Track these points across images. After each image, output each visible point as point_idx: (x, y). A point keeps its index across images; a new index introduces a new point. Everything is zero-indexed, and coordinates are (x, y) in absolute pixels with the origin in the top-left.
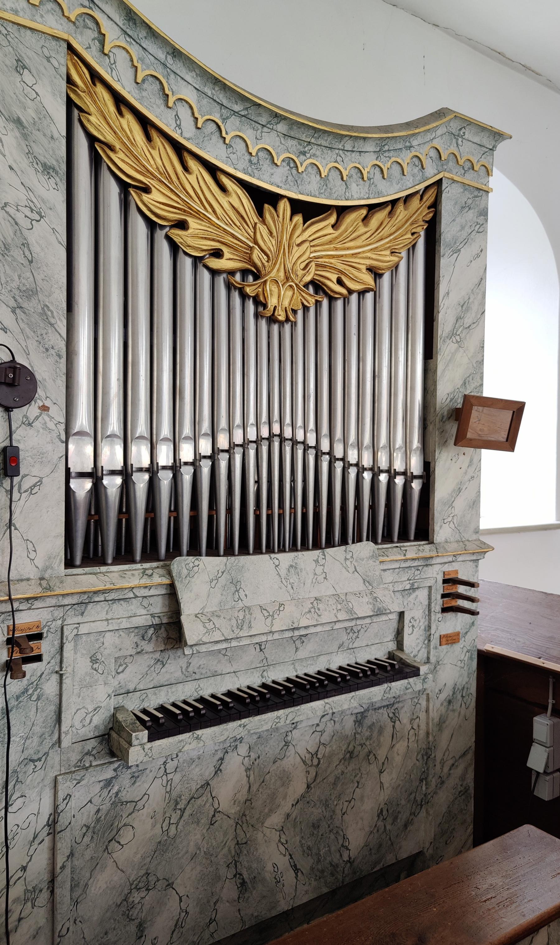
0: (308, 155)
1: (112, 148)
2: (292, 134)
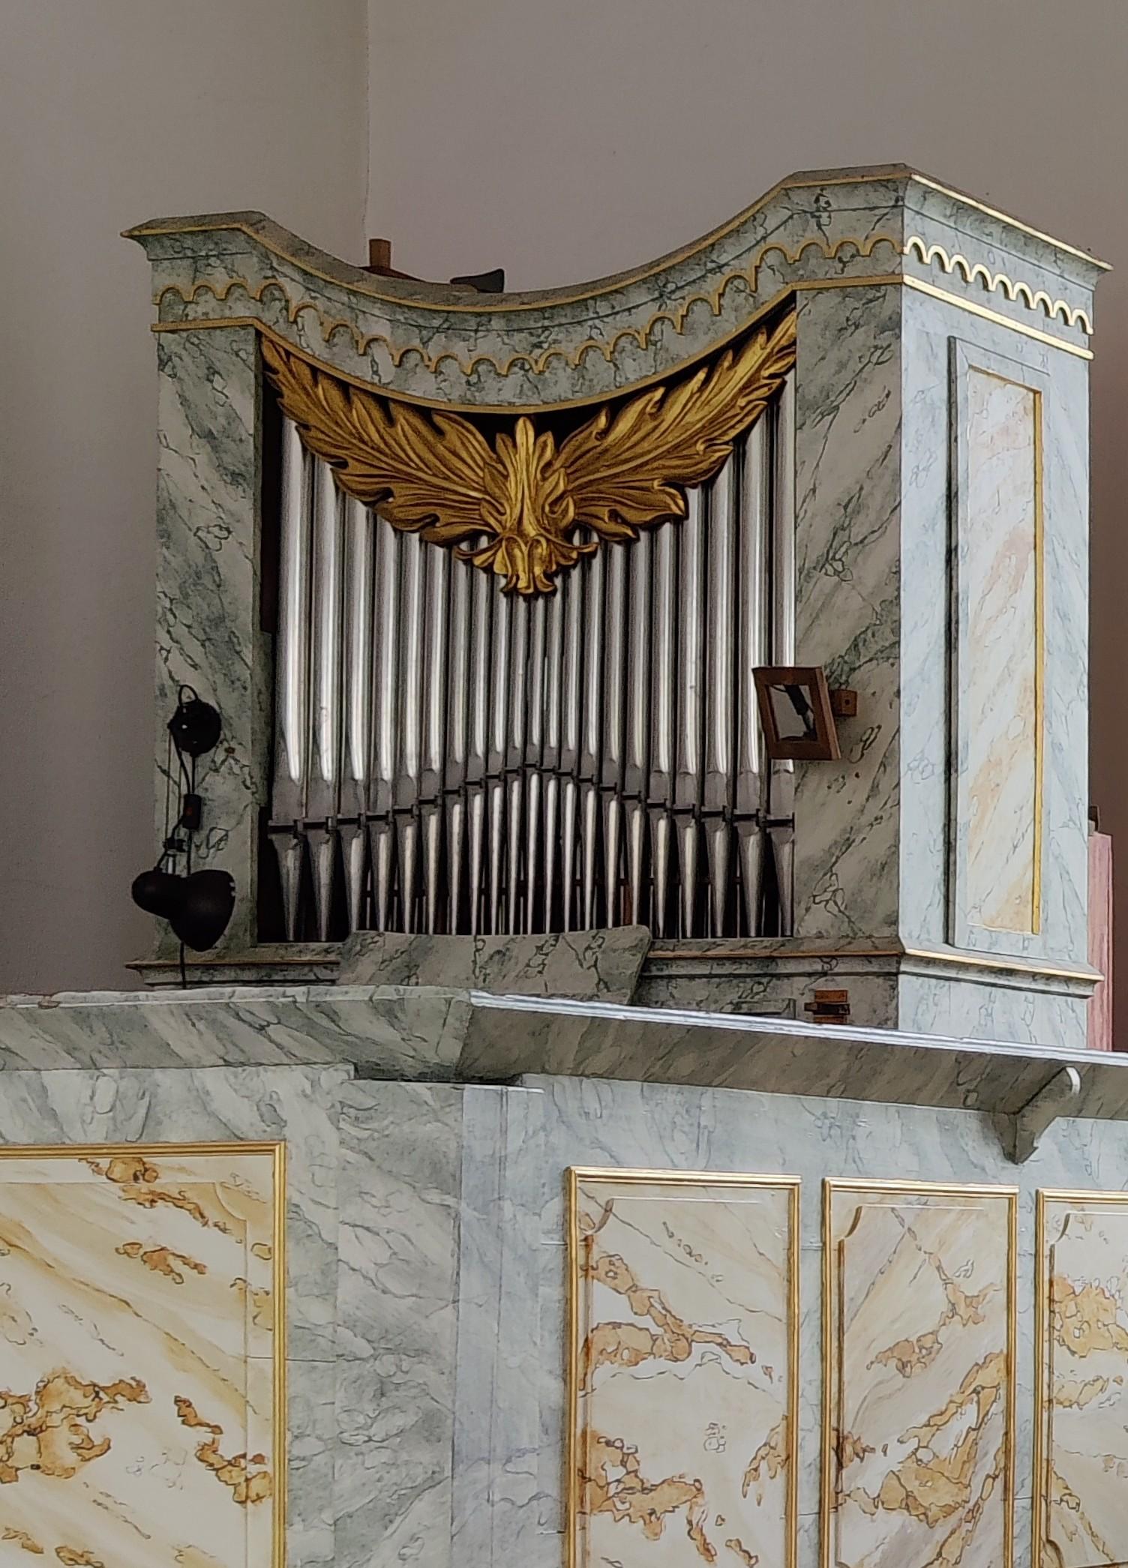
0: (545, 346)
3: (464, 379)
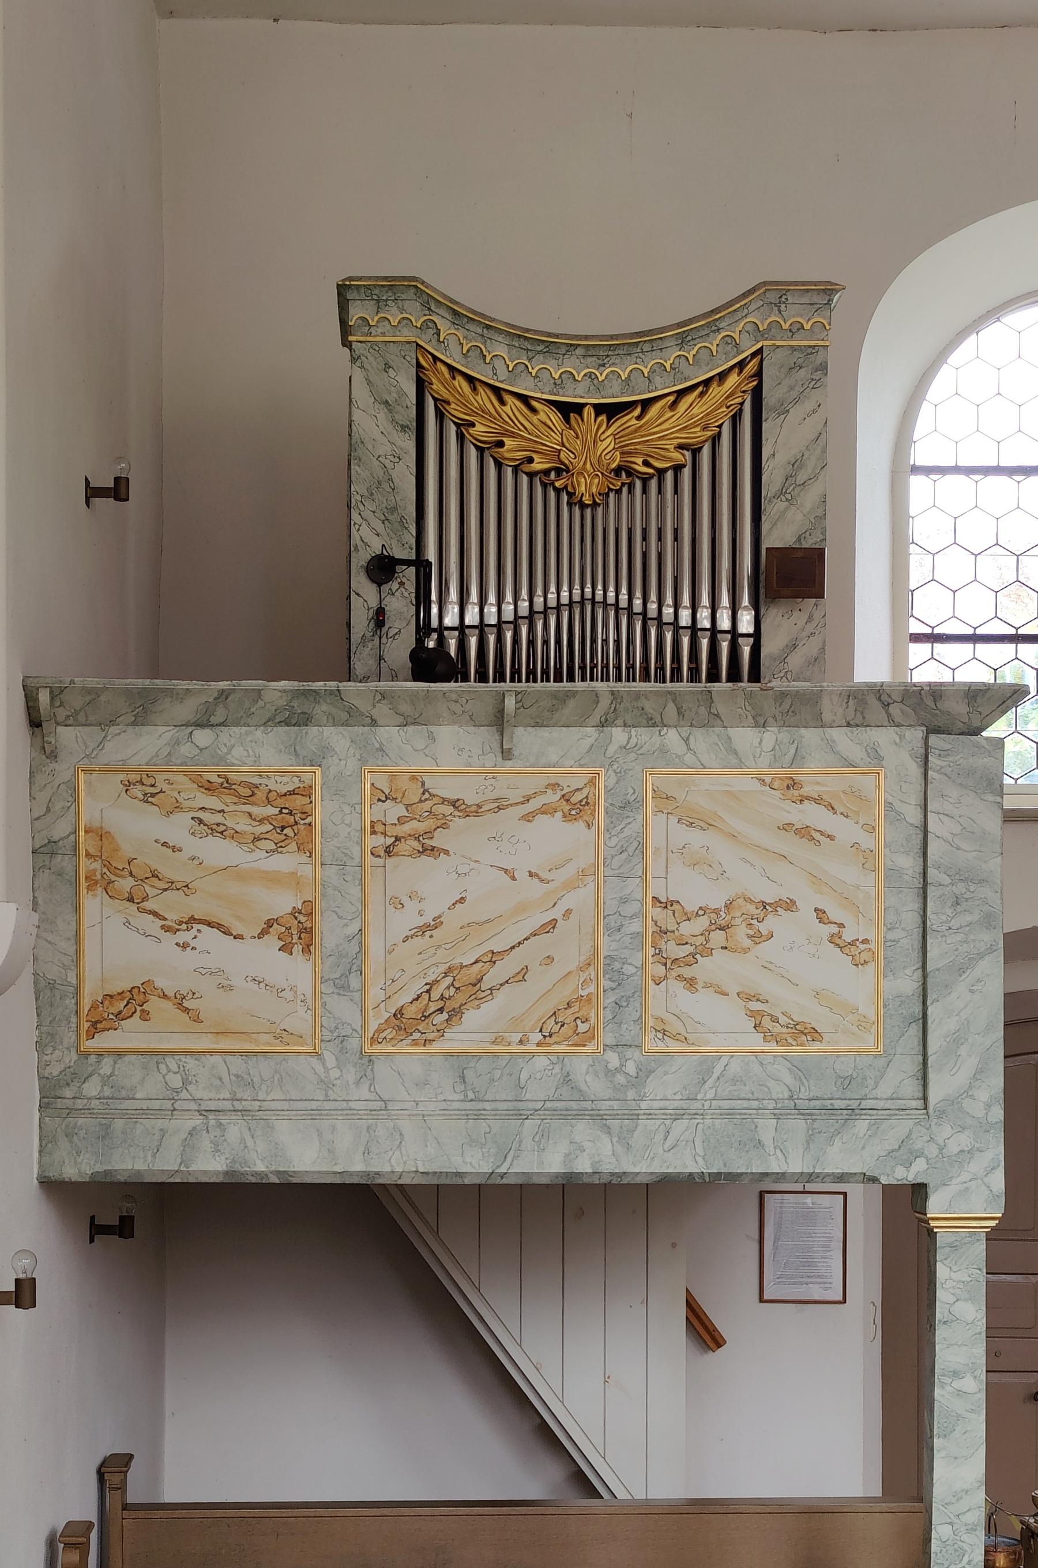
1: (449, 403)
2: (590, 353)
3: (552, 381)
